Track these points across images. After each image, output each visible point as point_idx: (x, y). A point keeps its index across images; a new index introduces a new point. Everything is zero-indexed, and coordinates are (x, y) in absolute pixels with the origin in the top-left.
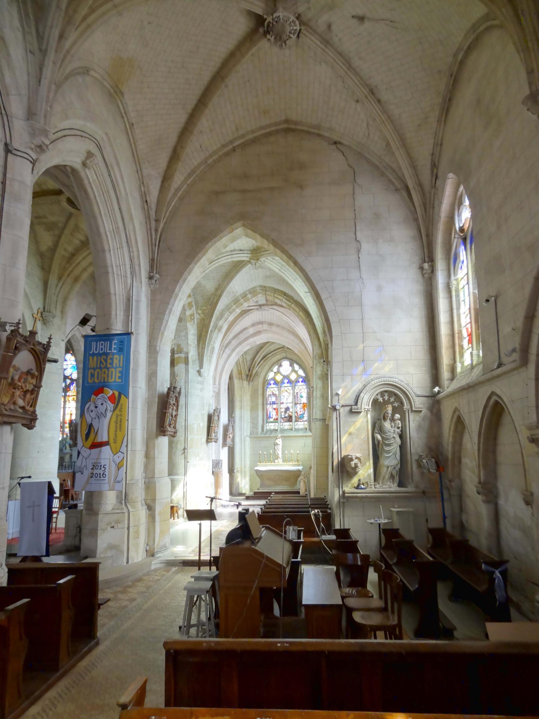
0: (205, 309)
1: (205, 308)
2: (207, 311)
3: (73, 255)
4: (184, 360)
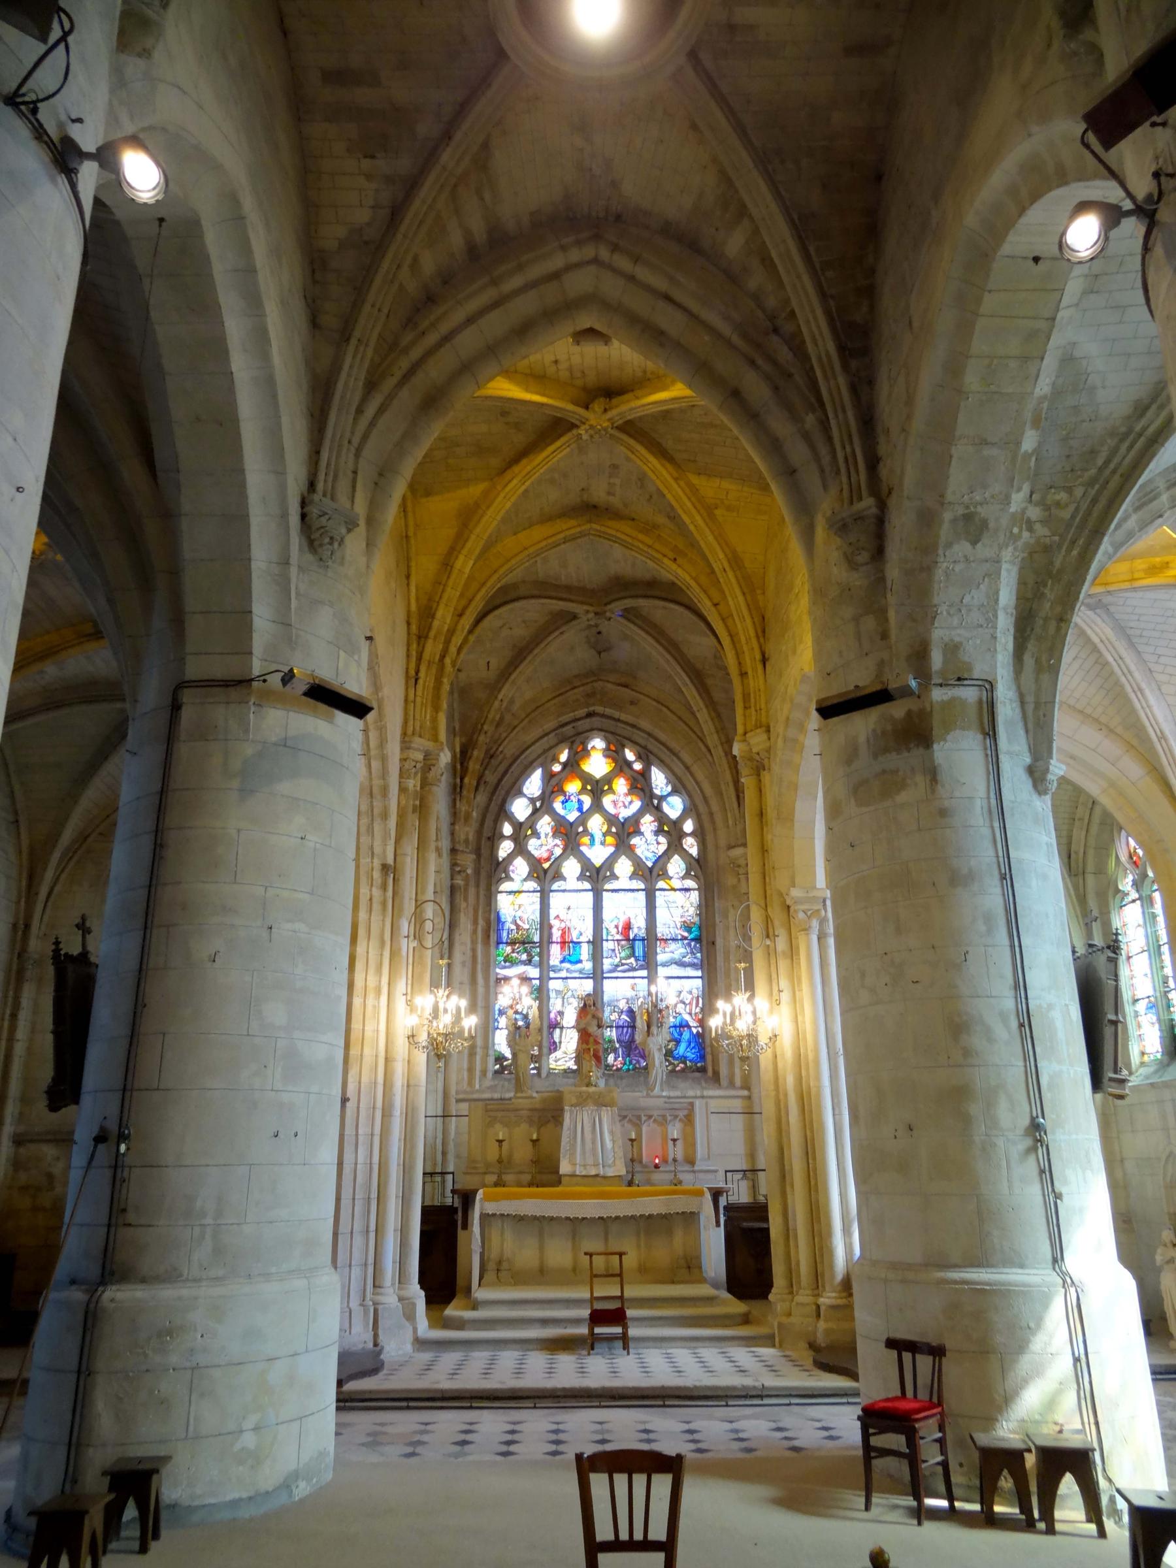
0: (1058, 504)
1: (1063, 496)
2: (1066, 514)
3: (430, 299)
4: (972, 713)
